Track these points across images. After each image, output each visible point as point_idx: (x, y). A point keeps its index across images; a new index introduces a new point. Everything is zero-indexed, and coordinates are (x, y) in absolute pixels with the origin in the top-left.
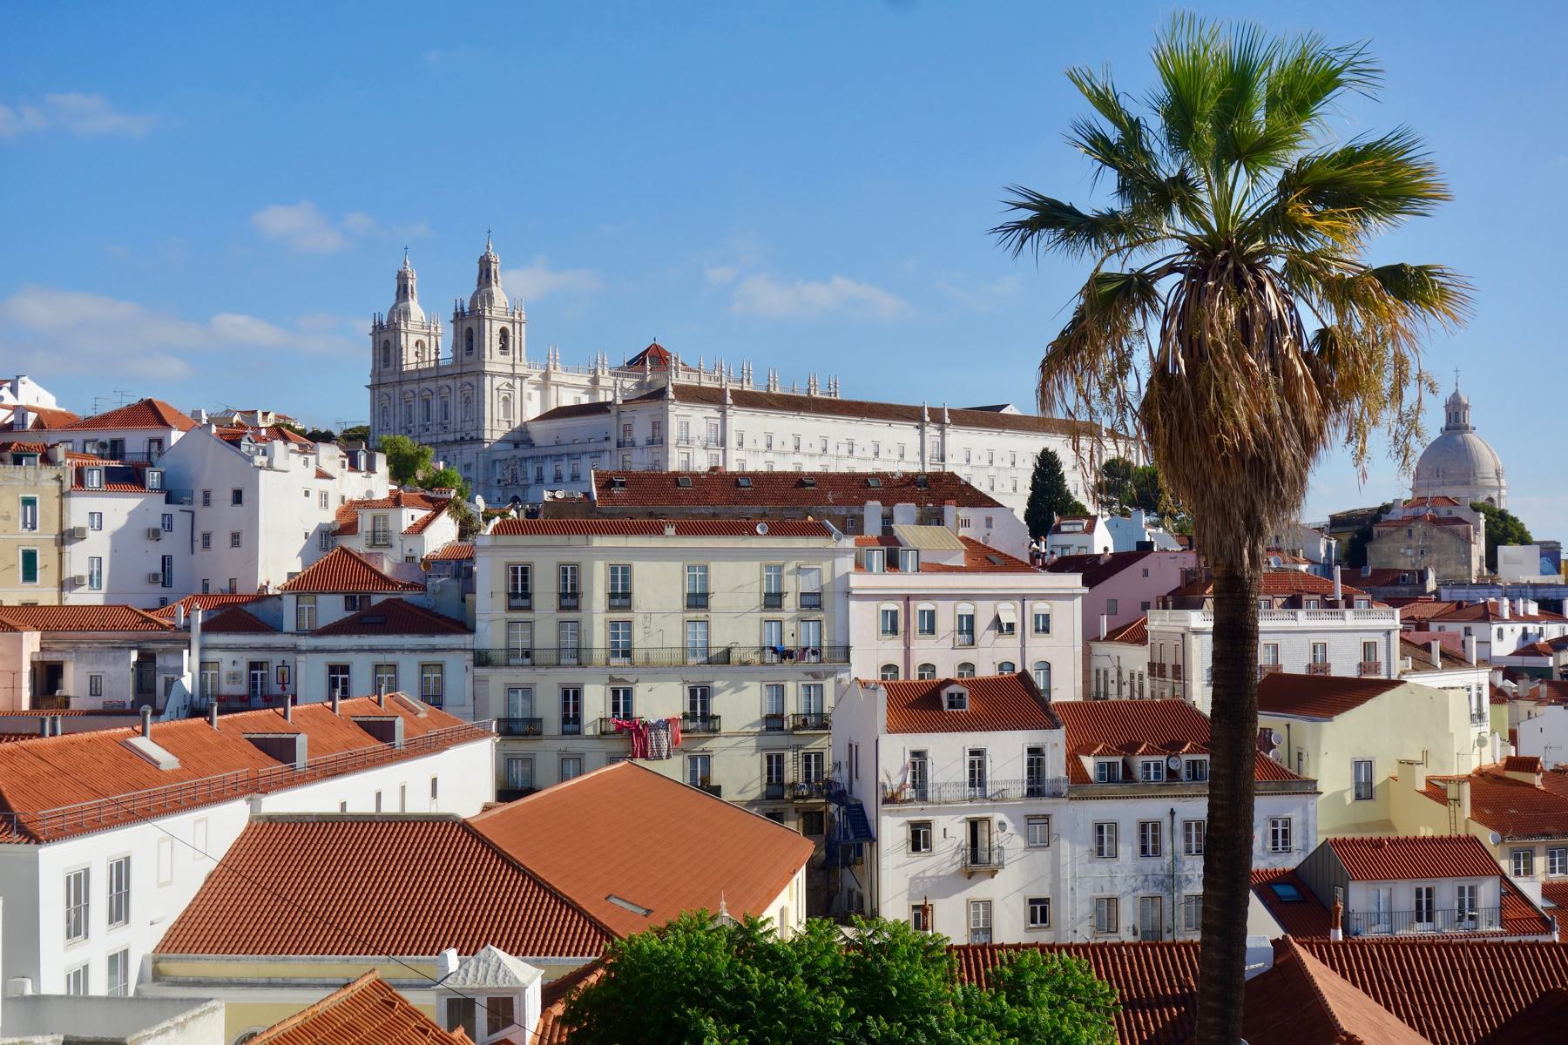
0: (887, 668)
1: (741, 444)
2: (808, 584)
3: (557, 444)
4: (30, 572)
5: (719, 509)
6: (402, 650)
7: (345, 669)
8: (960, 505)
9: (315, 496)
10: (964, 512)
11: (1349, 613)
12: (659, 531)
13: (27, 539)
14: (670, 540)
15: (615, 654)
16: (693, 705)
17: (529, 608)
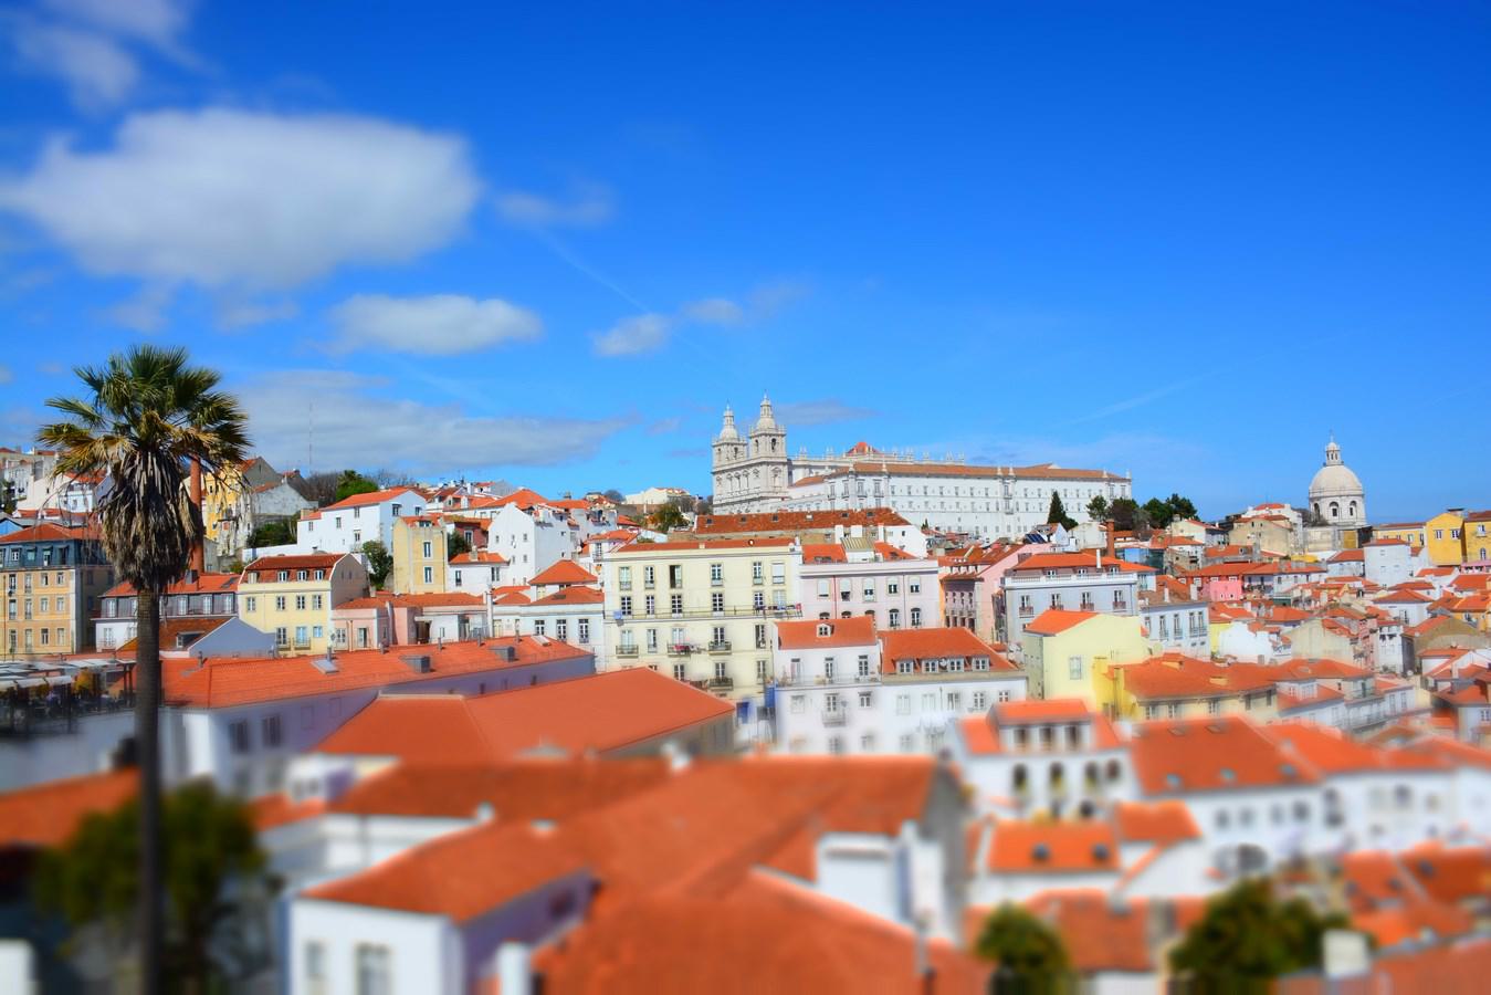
0: (822, 615)
1: (893, 493)
2: (778, 571)
3: (804, 497)
4: (428, 579)
5: (757, 533)
6: (569, 613)
7: (542, 622)
8: (885, 525)
9: (567, 535)
10: (889, 529)
11: (1104, 576)
12: (696, 546)
13: (427, 561)
14: (702, 550)
15: (674, 611)
16: (716, 637)
17: (630, 589)
